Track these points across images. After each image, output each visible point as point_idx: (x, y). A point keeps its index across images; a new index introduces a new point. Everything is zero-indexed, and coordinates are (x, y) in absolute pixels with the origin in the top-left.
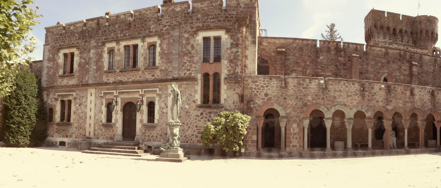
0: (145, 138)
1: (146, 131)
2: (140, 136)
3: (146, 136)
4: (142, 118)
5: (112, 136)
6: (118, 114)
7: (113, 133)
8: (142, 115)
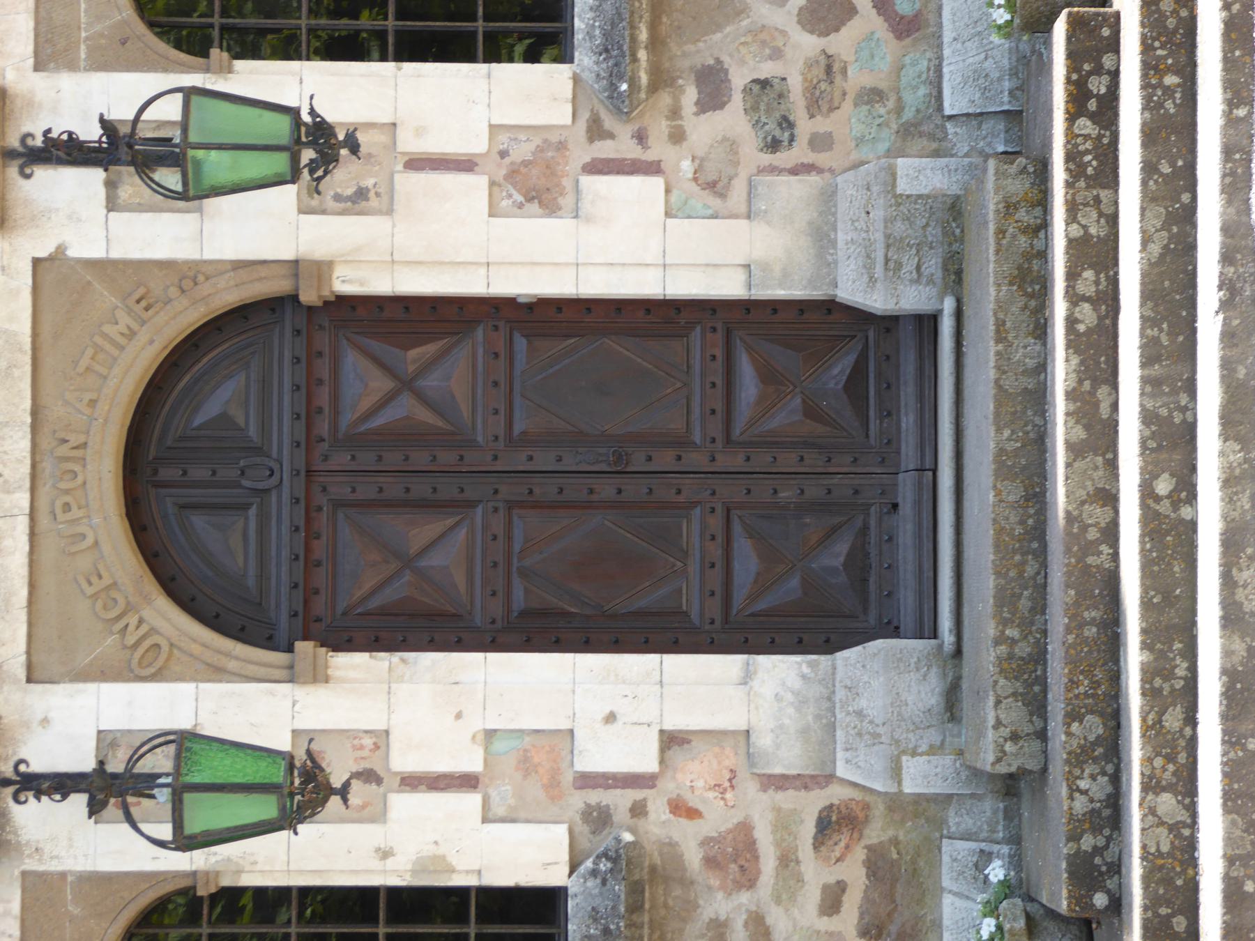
0: (873, 96)
1: (739, 78)
2: (828, 197)
3: (830, 67)
4: (464, 165)
5: (854, 872)
6: (382, 738)
7: (787, 860)
8: (417, 163)
